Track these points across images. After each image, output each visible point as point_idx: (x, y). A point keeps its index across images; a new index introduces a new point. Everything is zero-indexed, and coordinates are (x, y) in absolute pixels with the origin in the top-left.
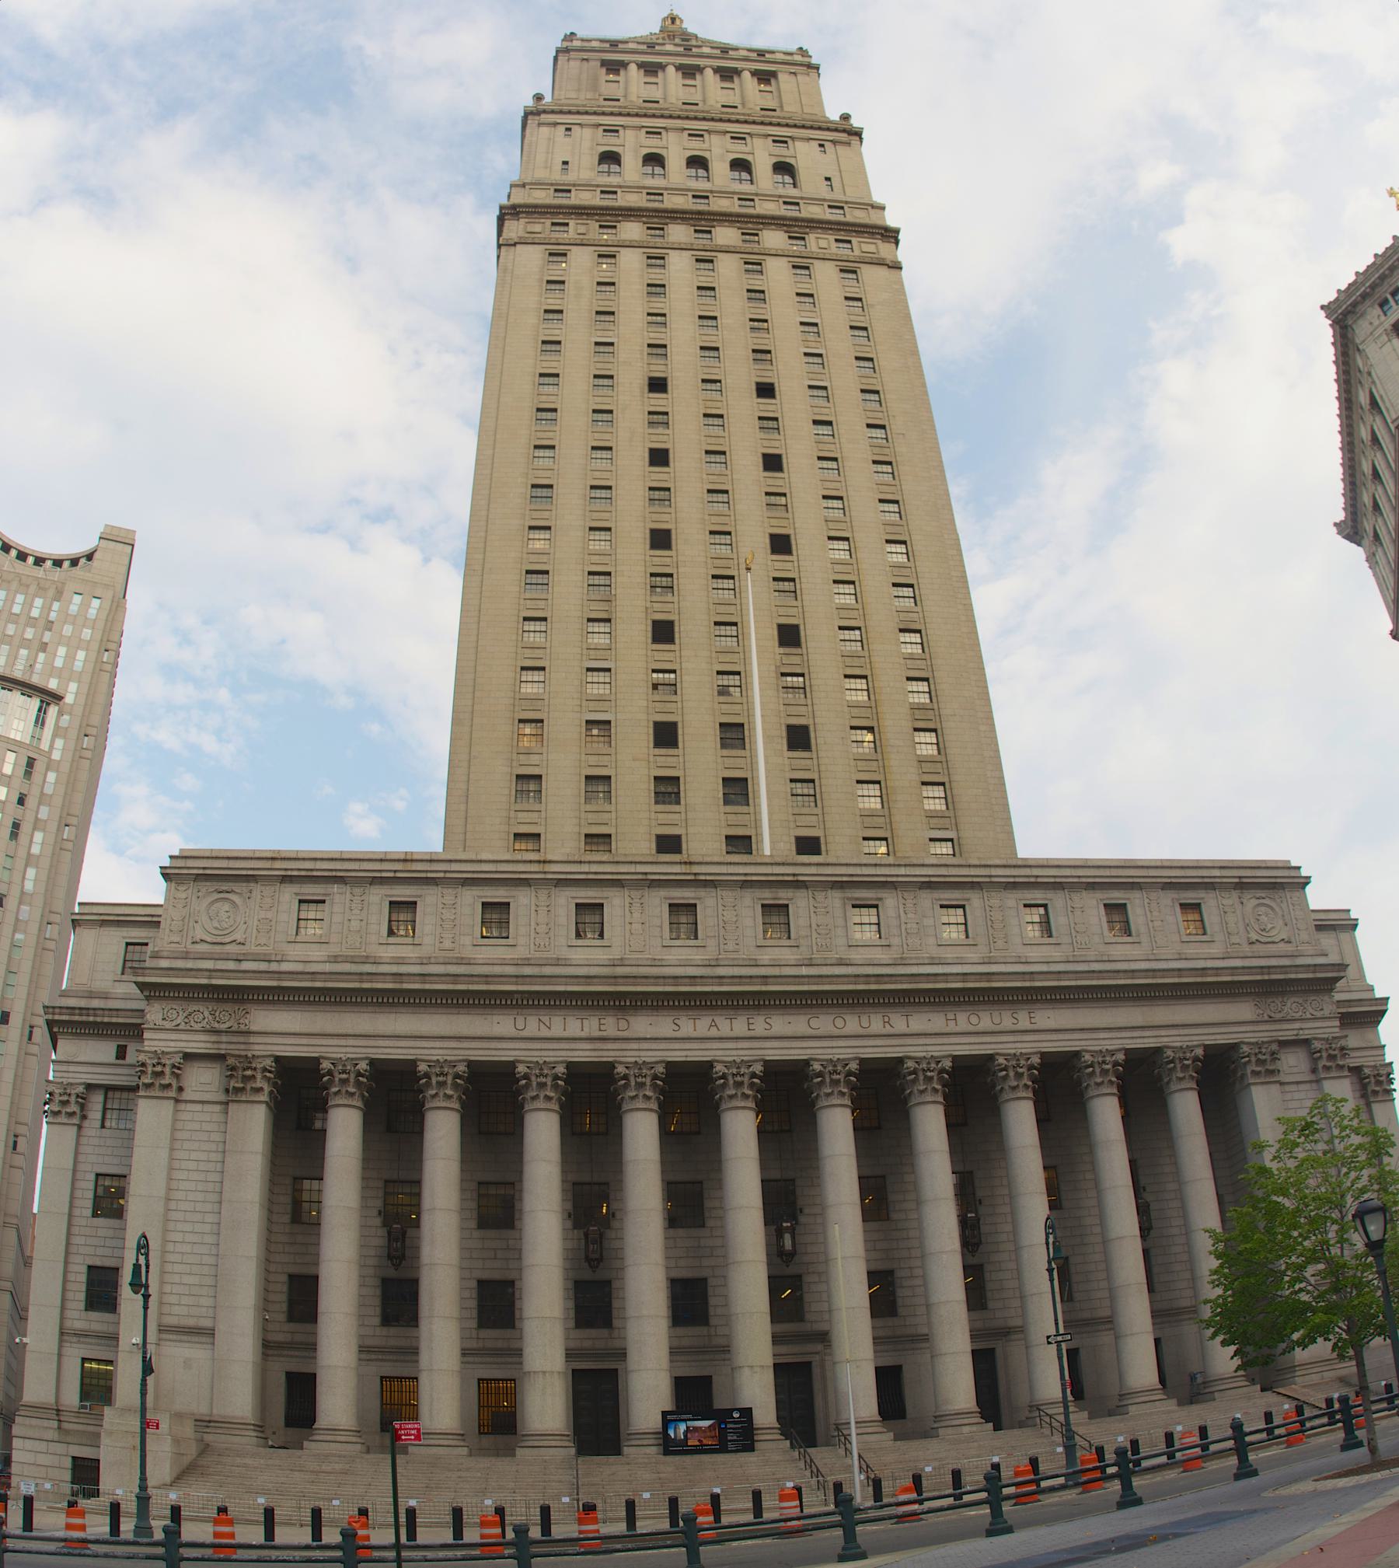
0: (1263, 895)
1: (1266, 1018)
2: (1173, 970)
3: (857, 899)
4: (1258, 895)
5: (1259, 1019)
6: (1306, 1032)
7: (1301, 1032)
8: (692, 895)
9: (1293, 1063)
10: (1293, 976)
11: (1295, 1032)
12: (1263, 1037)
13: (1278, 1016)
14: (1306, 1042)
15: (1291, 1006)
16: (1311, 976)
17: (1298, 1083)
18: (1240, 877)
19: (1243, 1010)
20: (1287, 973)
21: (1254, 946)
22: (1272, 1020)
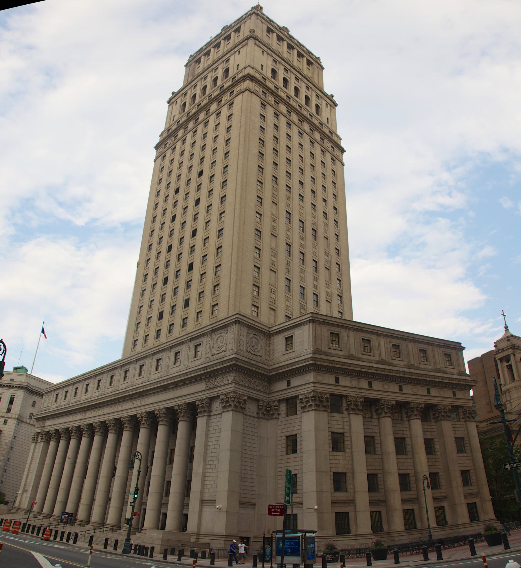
0: (221, 332)
1: (208, 388)
2: (177, 376)
3: (125, 369)
4: (219, 333)
5: (206, 389)
6: (221, 391)
7: (219, 392)
8: (101, 377)
9: (217, 406)
10: (215, 368)
11: (217, 393)
12: (204, 397)
13: (212, 387)
14: (218, 397)
15: (217, 382)
16: (221, 366)
17: (217, 415)
18: (212, 328)
19: (201, 386)
20: (212, 368)
21: (213, 356)
22: (211, 389)
